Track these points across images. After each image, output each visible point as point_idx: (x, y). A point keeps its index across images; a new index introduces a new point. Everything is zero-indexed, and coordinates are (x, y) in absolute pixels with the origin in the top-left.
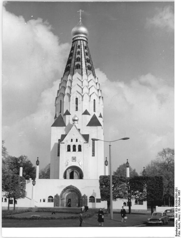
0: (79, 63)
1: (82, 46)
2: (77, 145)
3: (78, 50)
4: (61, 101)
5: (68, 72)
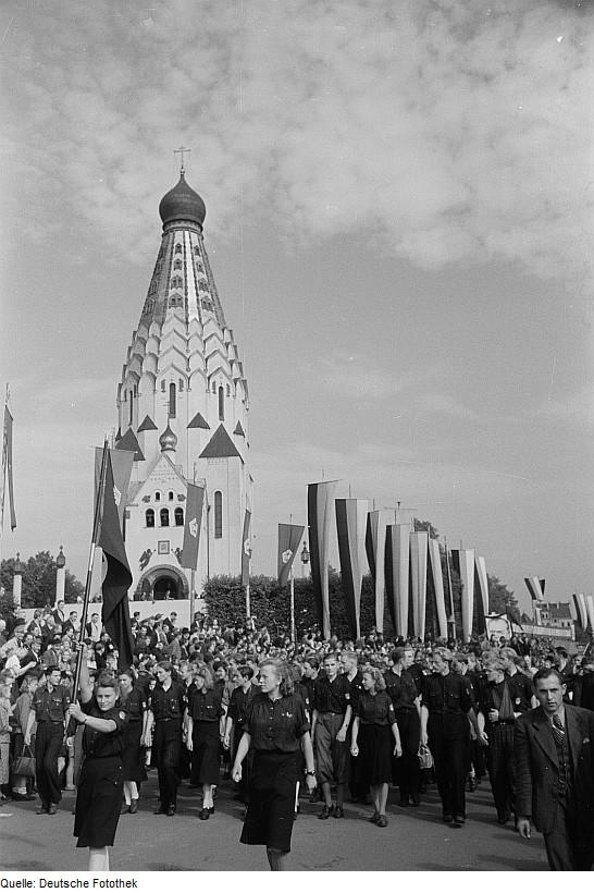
0: (181, 291)
1: (188, 245)
2: (172, 507)
3: (177, 256)
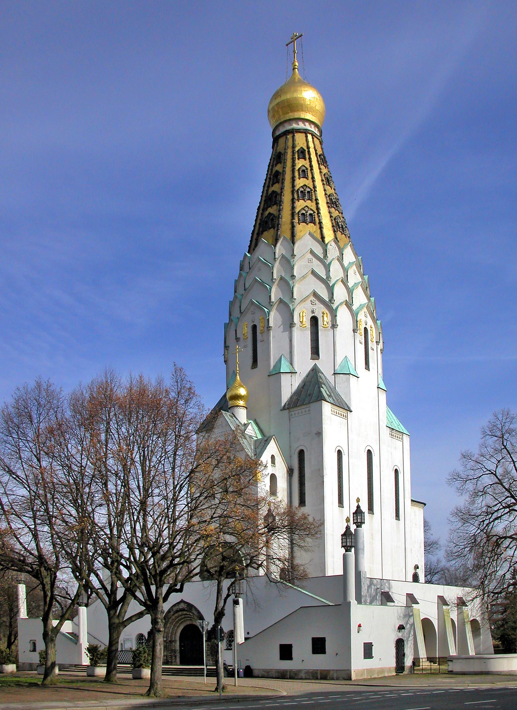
3: (300, 163)
4: (254, 328)
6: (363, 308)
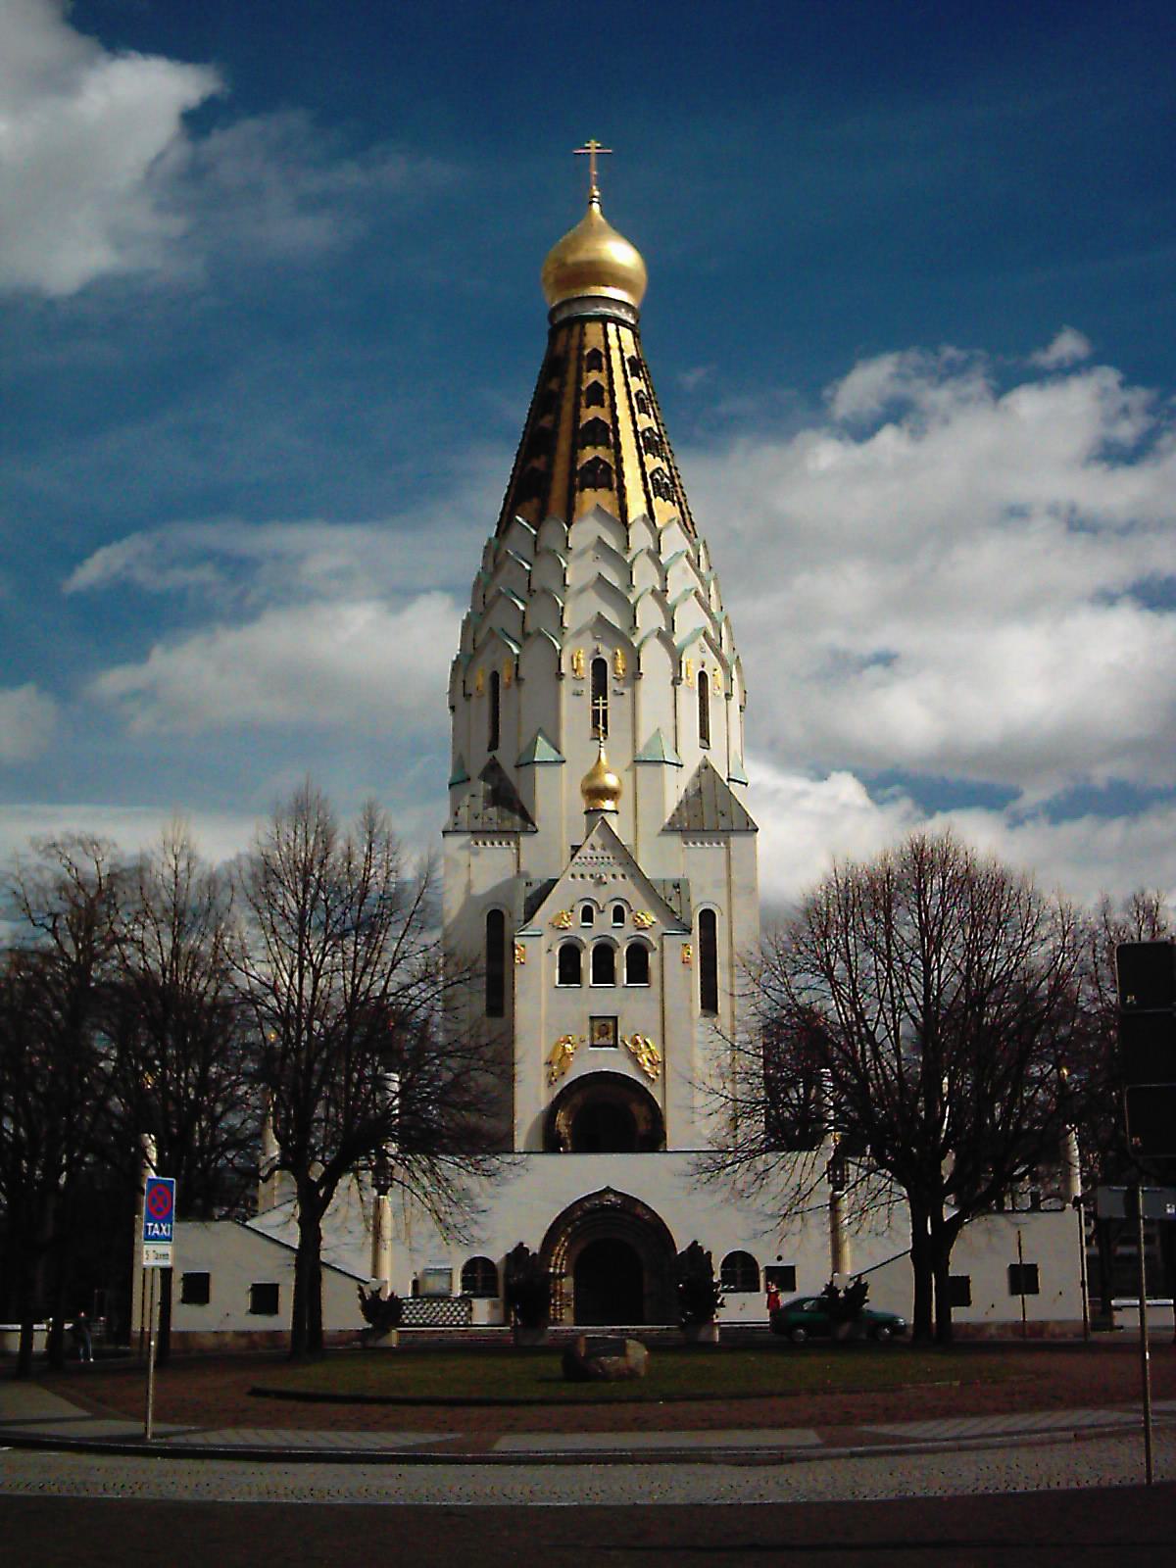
2: (622, 939)
5: (535, 501)
6: (697, 637)
